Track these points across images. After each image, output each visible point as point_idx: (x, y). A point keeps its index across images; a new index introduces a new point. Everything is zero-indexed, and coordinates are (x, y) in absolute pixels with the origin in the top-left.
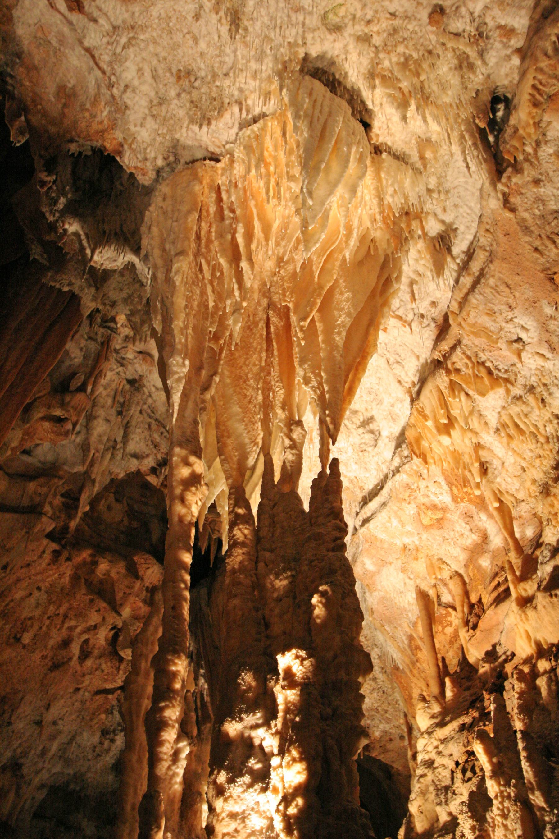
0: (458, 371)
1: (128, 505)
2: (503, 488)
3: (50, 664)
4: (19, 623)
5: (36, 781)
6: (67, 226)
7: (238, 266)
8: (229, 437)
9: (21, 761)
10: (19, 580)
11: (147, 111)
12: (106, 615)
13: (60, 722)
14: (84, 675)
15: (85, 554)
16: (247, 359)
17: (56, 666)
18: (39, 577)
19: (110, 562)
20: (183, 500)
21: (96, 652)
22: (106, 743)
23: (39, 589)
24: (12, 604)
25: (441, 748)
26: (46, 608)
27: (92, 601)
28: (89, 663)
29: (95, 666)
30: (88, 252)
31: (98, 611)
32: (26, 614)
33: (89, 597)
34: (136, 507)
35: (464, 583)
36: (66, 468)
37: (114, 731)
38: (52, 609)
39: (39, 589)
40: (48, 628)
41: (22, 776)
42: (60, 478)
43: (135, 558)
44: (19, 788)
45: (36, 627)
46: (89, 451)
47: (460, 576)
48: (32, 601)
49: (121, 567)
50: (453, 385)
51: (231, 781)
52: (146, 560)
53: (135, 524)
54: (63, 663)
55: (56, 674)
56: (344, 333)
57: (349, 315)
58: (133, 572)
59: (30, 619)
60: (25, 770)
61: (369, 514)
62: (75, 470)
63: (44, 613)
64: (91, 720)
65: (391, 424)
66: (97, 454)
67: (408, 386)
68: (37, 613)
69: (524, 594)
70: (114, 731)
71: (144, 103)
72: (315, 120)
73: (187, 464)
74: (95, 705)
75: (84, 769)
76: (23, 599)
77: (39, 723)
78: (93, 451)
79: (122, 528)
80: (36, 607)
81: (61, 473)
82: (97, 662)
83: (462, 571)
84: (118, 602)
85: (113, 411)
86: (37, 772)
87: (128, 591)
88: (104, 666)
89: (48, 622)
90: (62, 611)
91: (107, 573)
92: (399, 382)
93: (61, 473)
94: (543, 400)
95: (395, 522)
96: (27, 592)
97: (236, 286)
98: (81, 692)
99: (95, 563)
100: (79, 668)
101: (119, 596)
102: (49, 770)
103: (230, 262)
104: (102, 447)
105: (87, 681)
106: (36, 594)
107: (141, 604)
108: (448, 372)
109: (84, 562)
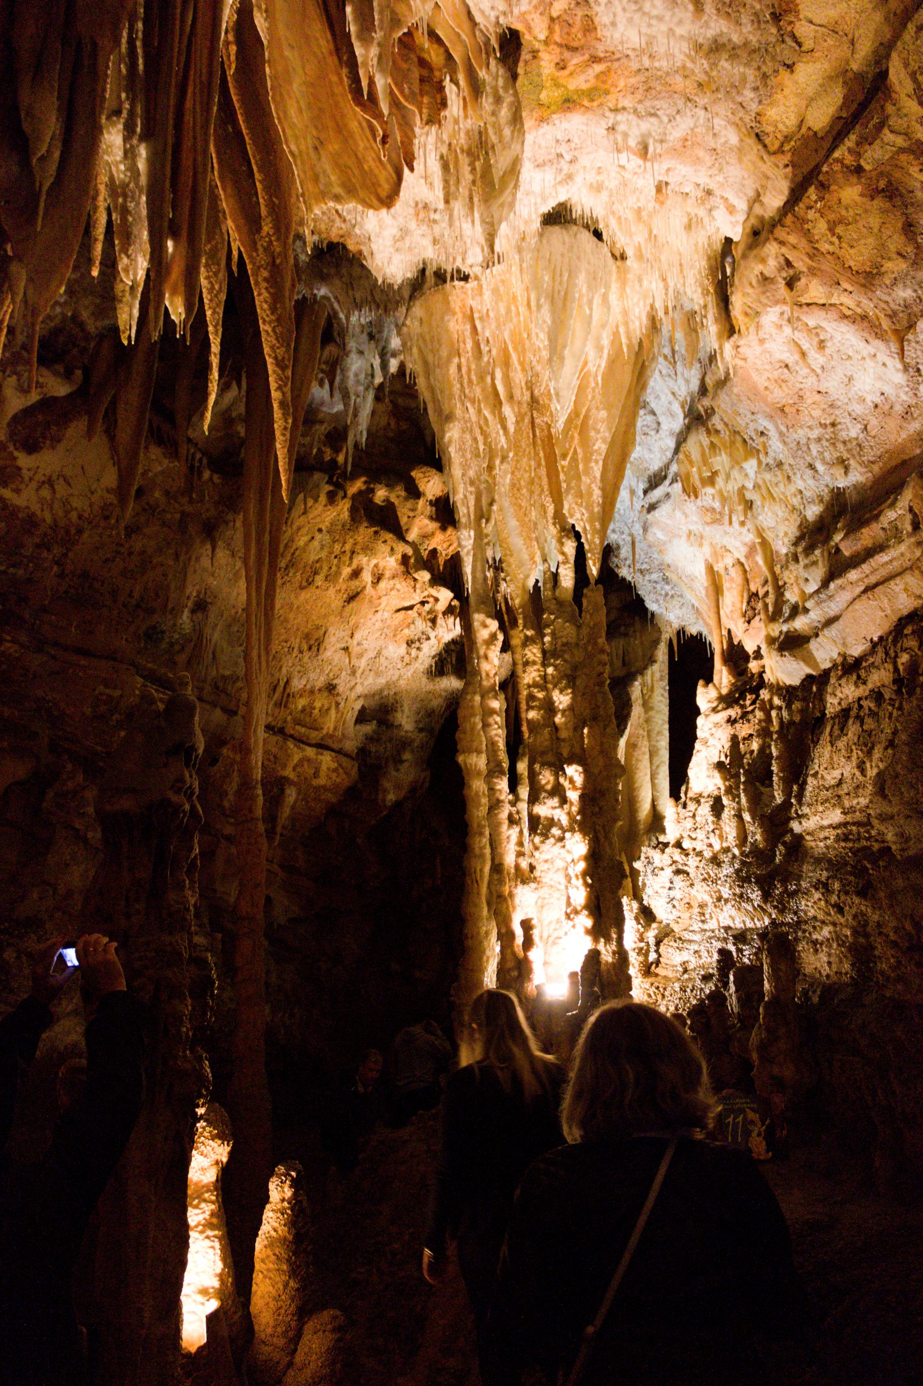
0: (717, 432)
1: (391, 401)
2: (765, 525)
3: (345, 596)
4: (308, 568)
5: (353, 695)
6: (316, 291)
7: (500, 413)
8: (511, 555)
9: (335, 682)
10: (299, 529)
11: (392, 250)
12: (395, 546)
13: (364, 642)
14: (380, 598)
15: (358, 485)
16: (518, 461)
17: (352, 598)
18: (318, 519)
19: (387, 486)
20: (486, 657)
21: (388, 574)
22: (414, 652)
23: (320, 530)
24: (297, 553)
25: (714, 730)
26: (332, 547)
27: (376, 533)
28: (383, 585)
29: (389, 587)
30: (342, 316)
31: (385, 542)
32: (313, 557)
33: (373, 529)
34: (400, 401)
35: (745, 571)
36: (324, 409)
37: (419, 640)
38: (337, 547)
39: (320, 530)
40: (338, 567)
41: (338, 694)
42: (322, 422)
43: (413, 474)
44: (338, 704)
45: (325, 569)
46: (349, 397)
47: (742, 564)
48: (316, 544)
49: (400, 491)
50: (713, 446)
51: (543, 842)
52: (424, 473)
53: (404, 426)
54: (358, 593)
55: (353, 604)
56: (601, 463)
57: (604, 441)
58: (414, 493)
59: (317, 561)
60: (340, 689)
61: (654, 500)
62: (335, 410)
63: (331, 553)
64: (395, 636)
65: (670, 419)
66: (358, 400)
67: (681, 399)
68: (323, 554)
69: (773, 634)
70: (419, 640)
71: (389, 242)
72: (556, 296)
73: (485, 626)
74: (396, 622)
75: (394, 678)
76: (306, 544)
77: (346, 649)
78: (353, 398)
79: (391, 434)
80: (322, 548)
81: (321, 416)
82: (392, 582)
83: (743, 560)
84: (404, 528)
85: (364, 337)
86: (352, 689)
87: (411, 514)
88: (398, 586)
89: (336, 561)
90: (348, 547)
91: (387, 500)
92: (673, 394)
93: (321, 416)
94: (789, 477)
95: (678, 514)
96: (309, 536)
97: (501, 432)
98: (380, 613)
99: (372, 491)
100: (373, 592)
101: (403, 520)
102: (362, 684)
103: (493, 413)
104: (361, 388)
105: (384, 600)
106: (318, 536)
107: (427, 521)
108: (708, 432)
109: (360, 492)
